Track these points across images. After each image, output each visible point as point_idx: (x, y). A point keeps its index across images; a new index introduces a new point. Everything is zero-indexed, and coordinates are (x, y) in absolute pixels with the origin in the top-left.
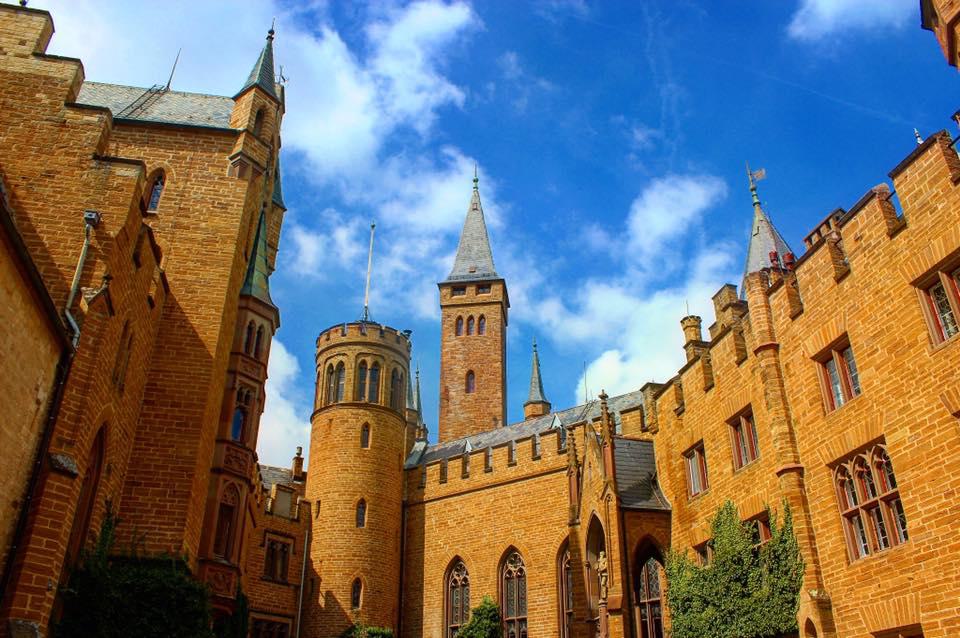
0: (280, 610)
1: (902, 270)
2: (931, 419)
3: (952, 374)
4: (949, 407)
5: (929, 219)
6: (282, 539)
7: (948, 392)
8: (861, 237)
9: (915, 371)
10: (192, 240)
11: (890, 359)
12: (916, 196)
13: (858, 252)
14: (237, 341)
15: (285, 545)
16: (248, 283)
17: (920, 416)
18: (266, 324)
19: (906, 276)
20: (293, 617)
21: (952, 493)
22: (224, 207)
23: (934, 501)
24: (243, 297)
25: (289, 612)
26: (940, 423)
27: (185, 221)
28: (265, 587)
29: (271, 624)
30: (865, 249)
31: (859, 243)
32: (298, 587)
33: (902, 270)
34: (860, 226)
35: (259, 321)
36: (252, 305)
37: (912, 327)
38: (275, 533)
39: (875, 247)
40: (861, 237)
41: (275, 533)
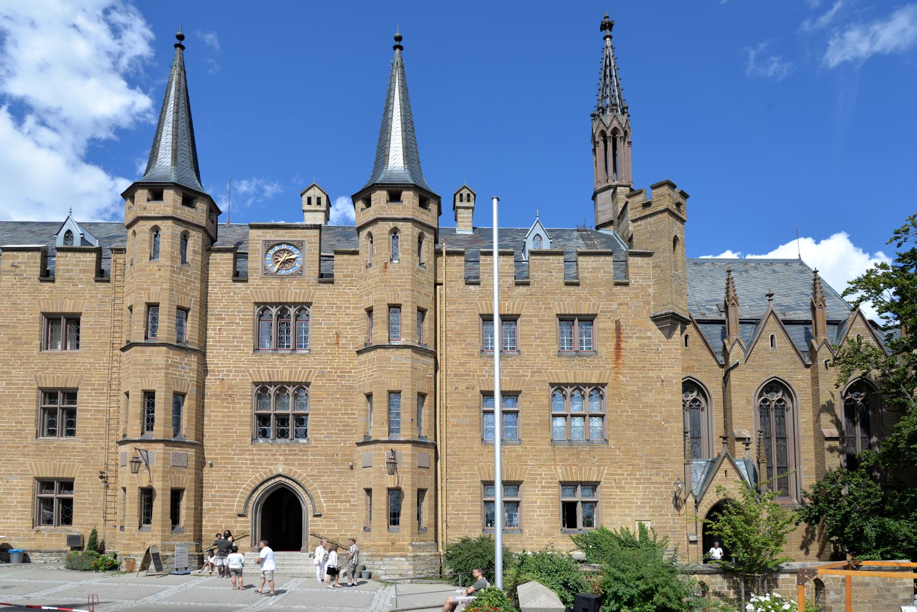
1: (39, 302)
2: (22, 384)
3: (47, 369)
4: (37, 382)
5: (69, 288)
7: (40, 376)
8: (17, 267)
9: (23, 357)
11: (6, 343)
12: (68, 271)
13: (12, 273)
17: (15, 380)
19: (40, 306)
21: (21, 423)
23: (7, 422)
26: (27, 389)
30: (17, 275)
31: (13, 269)
33: (39, 302)
34: (19, 260)
37: (31, 335)
39: (25, 278)
40: (17, 267)
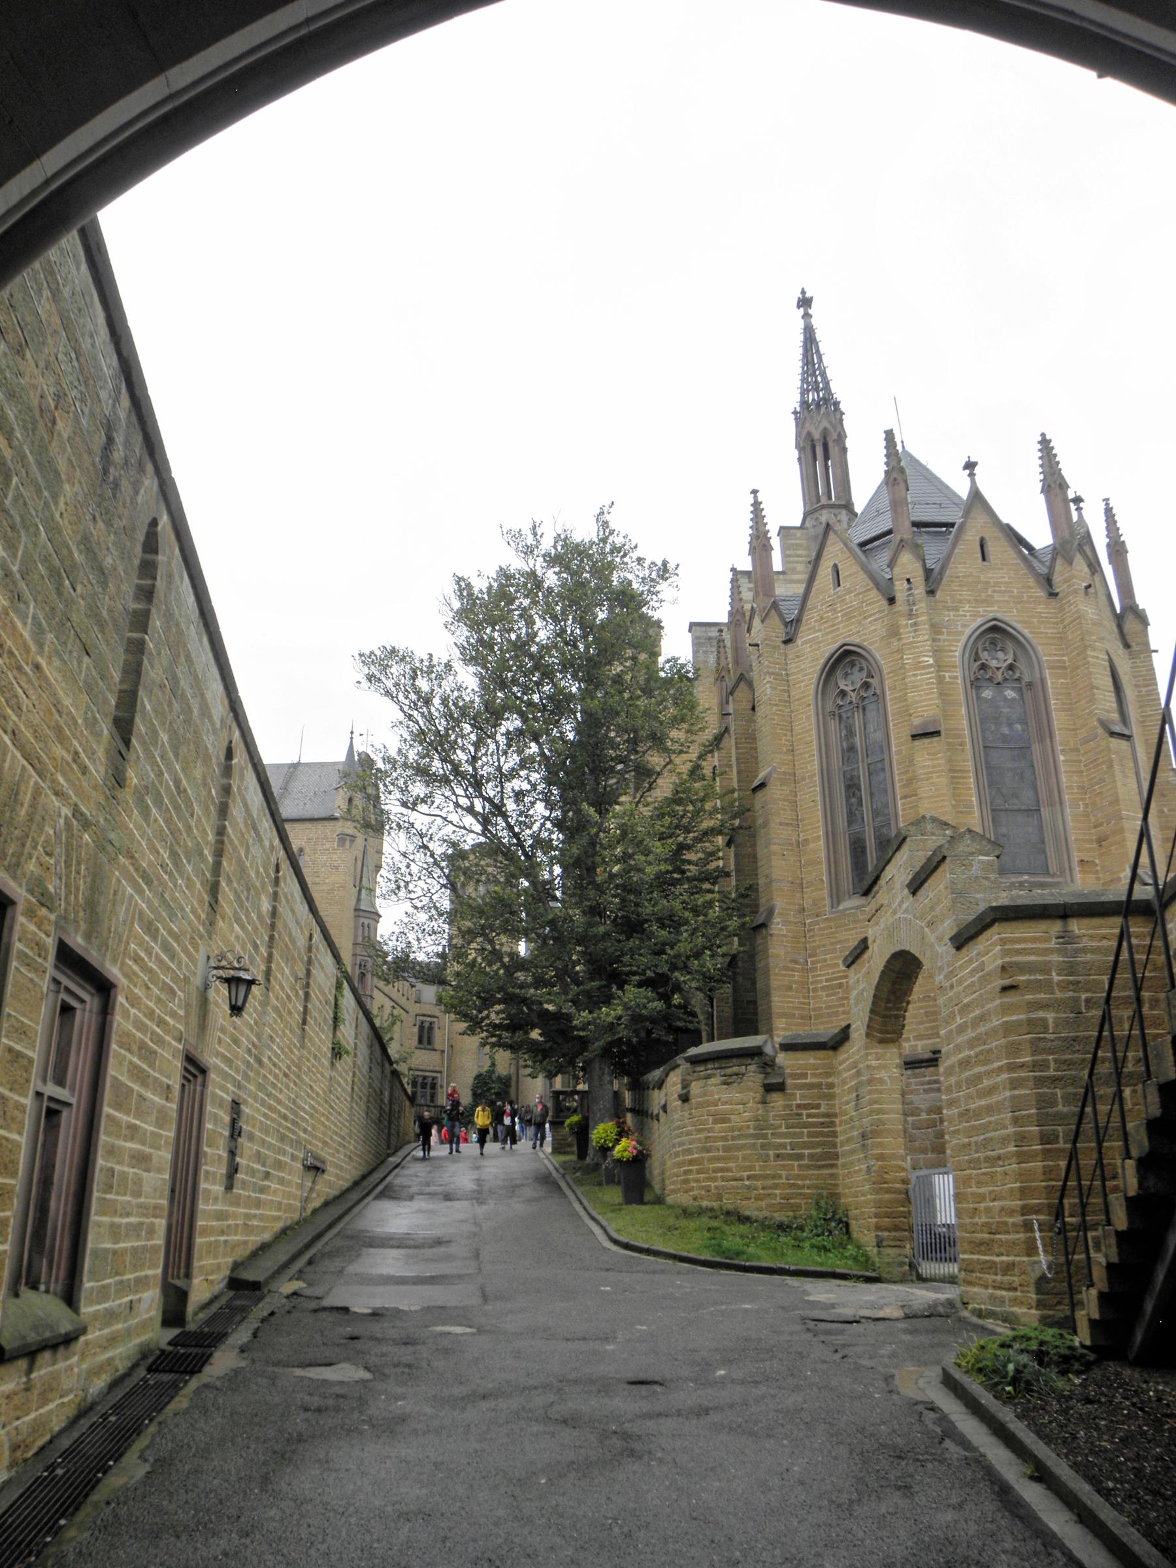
0: (431, 1068)
6: (429, 1019)
10: (322, 891)
14: (356, 936)
15: (431, 1023)
16: (359, 900)
18: (371, 922)
20: (440, 1072)
22: (337, 868)
24: (356, 910)
25: (437, 1069)
27: (317, 880)
28: (419, 1053)
29: (425, 1078)
32: (443, 1051)
35: (366, 922)
36: (361, 914)
38: (424, 1015)
41: (424, 1015)
